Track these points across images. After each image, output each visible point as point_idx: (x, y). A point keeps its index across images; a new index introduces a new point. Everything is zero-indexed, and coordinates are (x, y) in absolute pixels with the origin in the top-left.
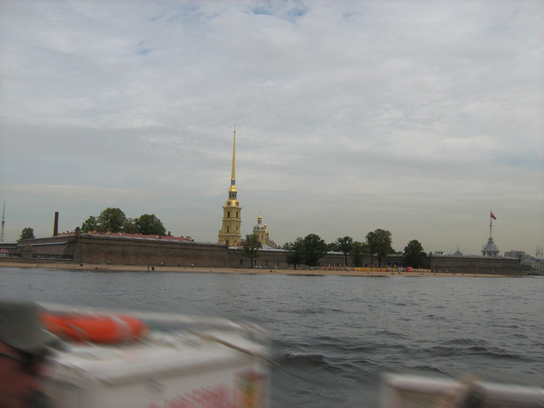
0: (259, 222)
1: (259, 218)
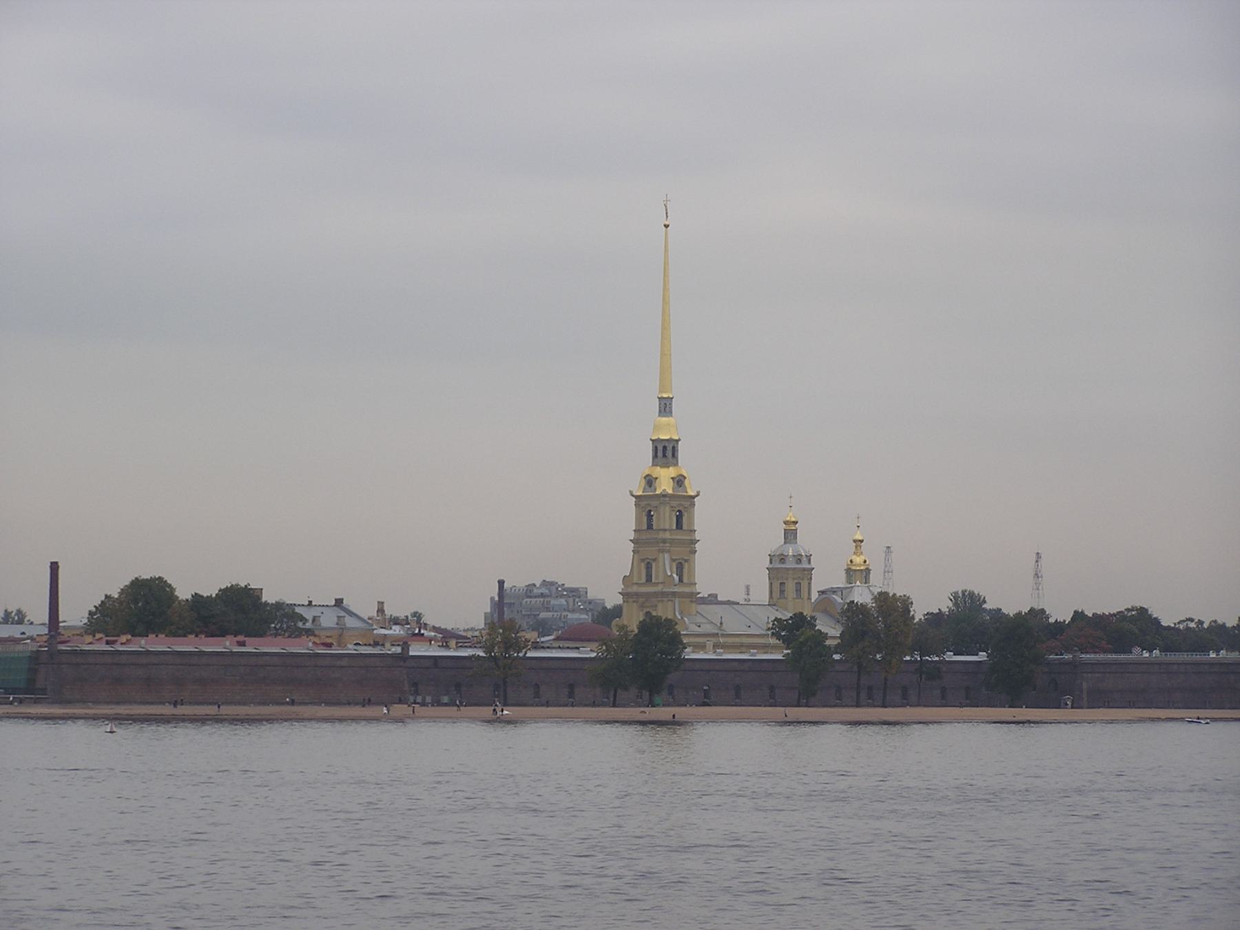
0: (790, 534)
1: (785, 523)
